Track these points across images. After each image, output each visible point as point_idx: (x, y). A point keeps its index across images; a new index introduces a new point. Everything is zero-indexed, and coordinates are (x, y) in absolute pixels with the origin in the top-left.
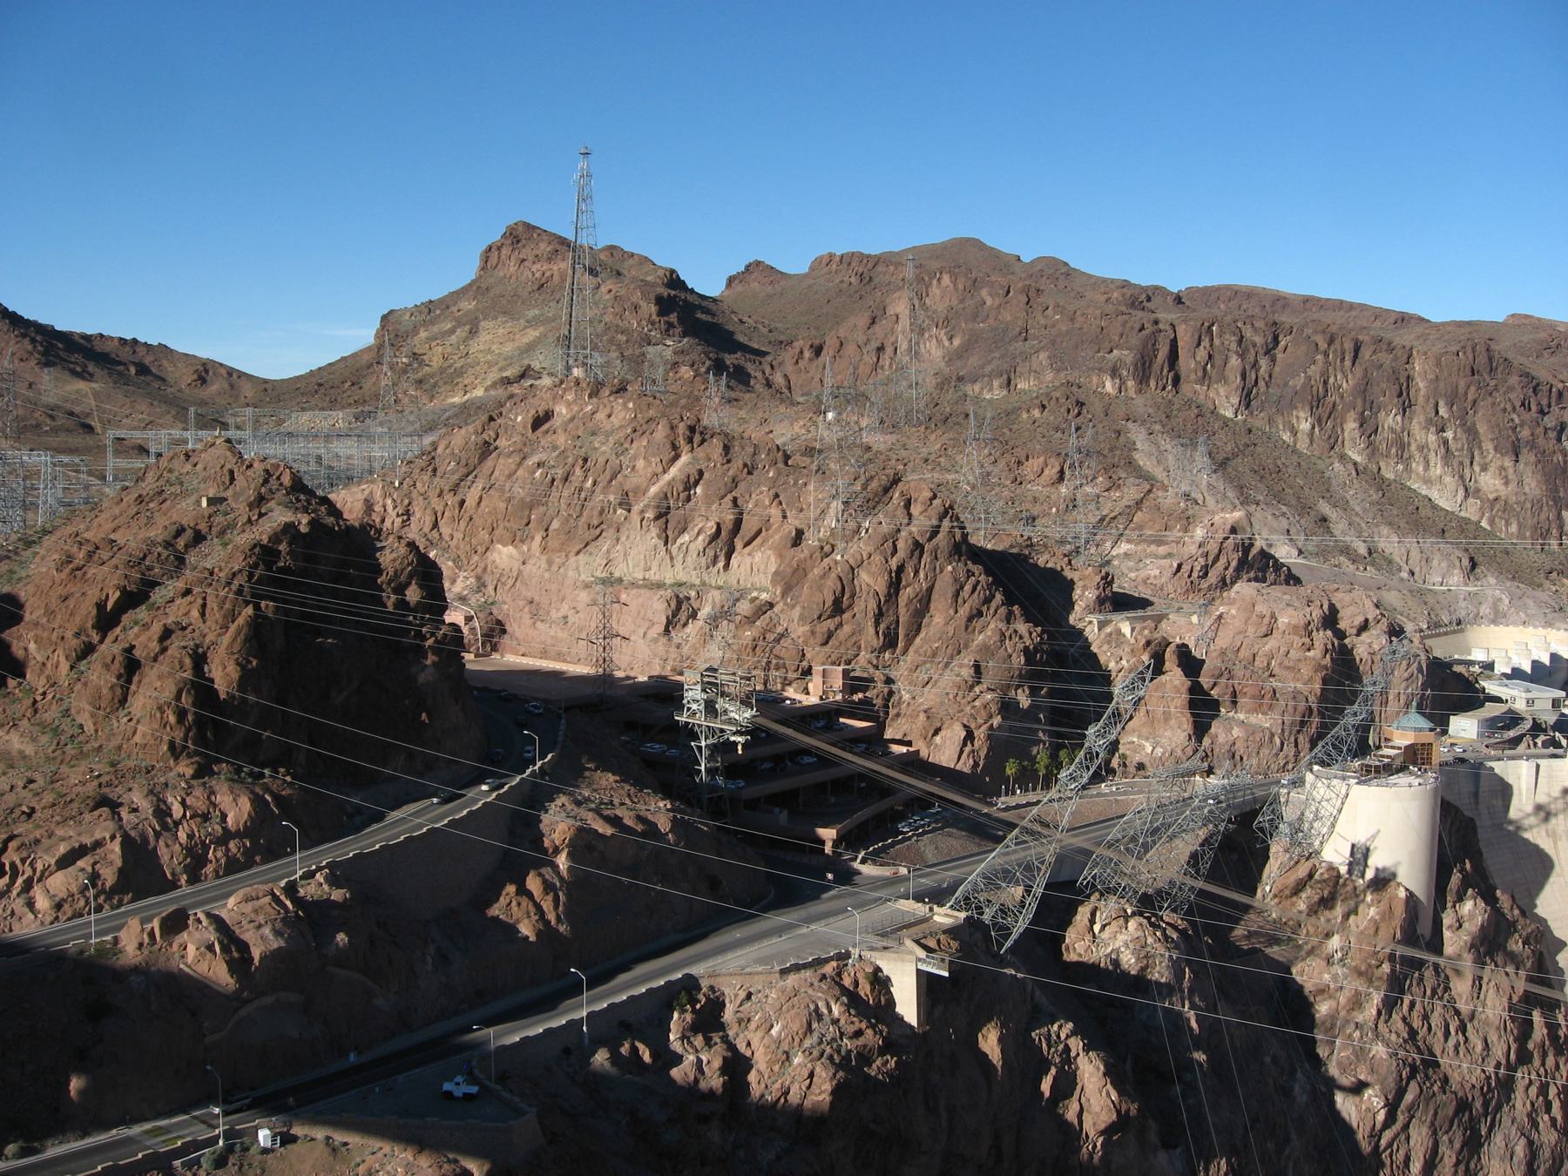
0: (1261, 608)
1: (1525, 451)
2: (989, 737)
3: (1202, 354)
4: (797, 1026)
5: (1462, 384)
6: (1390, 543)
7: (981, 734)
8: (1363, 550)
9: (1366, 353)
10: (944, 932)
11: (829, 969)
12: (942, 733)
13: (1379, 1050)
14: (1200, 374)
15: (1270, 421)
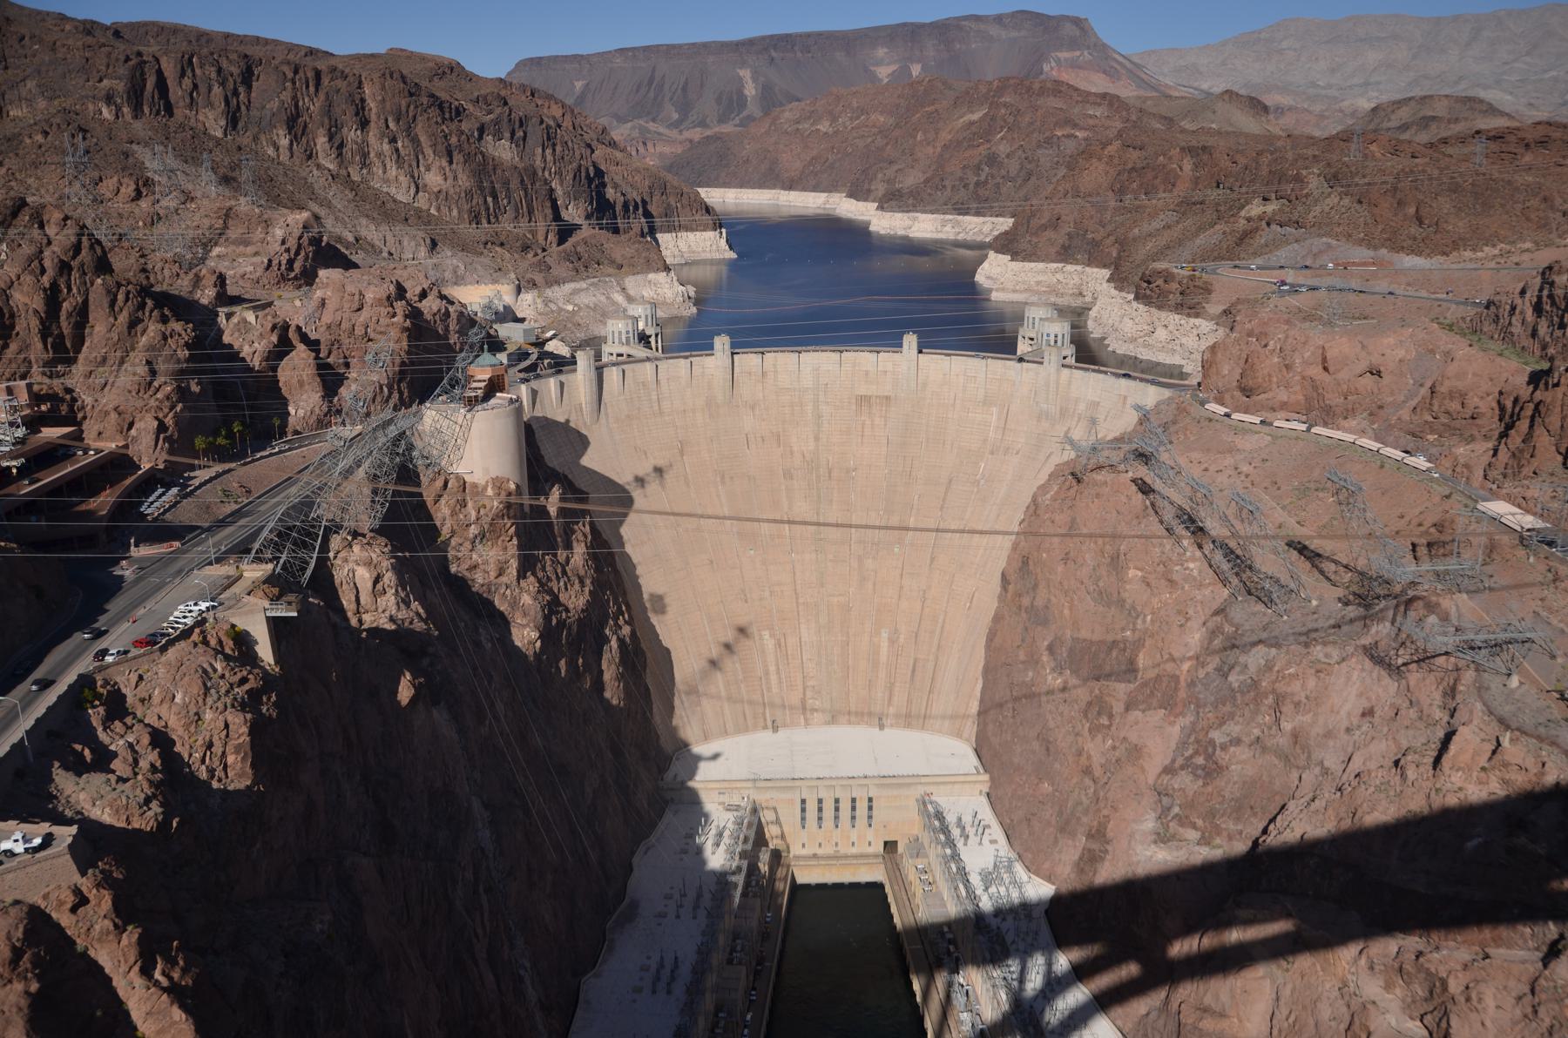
0: (350, 288)
1: (455, 153)
2: (176, 424)
3: (187, 82)
4: (196, 688)
5: (404, 103)
6: (371, 232)
7: (169, 421)
8: (351, 239)
9: (325, 81)
10: (264, 582)
11: (195, 637)
12: (136, 426)
13: (526, 599)
14: (188, 100)
15: (256, 139)
